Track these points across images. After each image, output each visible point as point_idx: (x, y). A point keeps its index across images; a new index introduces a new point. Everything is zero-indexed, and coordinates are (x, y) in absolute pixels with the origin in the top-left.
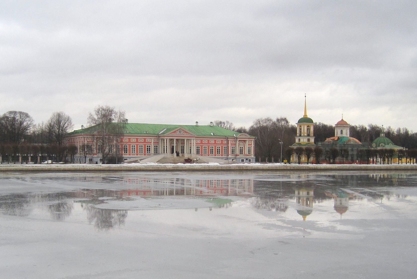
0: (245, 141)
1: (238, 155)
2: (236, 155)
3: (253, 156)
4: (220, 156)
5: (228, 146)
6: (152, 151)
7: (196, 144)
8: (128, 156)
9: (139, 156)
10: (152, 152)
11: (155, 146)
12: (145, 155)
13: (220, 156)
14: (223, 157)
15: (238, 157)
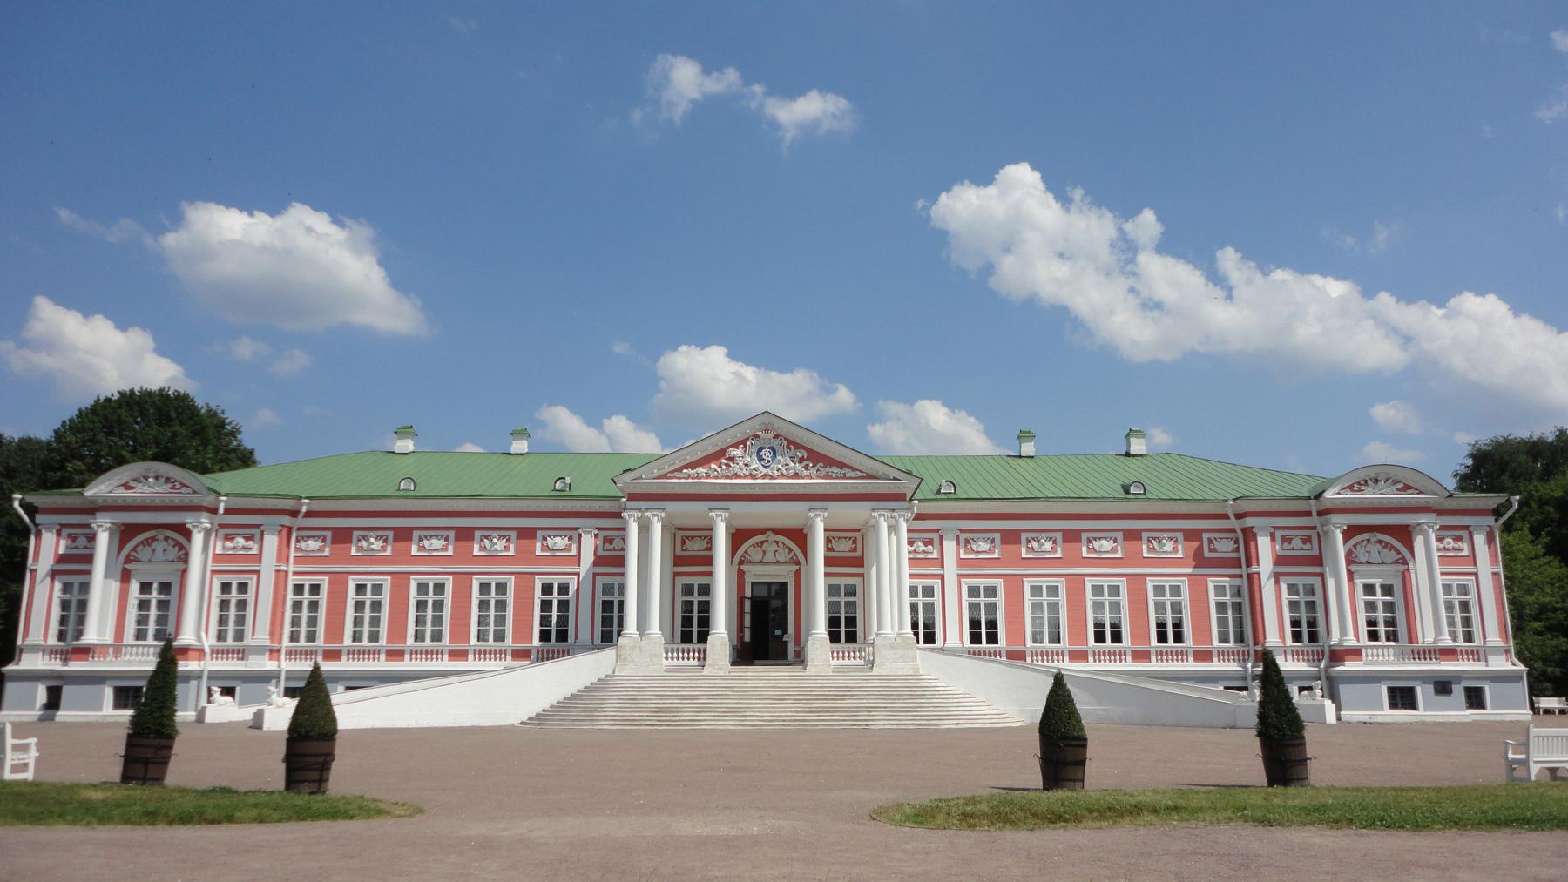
0: (1404, 534)
1: (1356, 653)
2: (1337, 655)
3: (1501, 663)
4: (1191, 666)
5: (1252, 579)
6: (584, 621)
7: (962, 563)
8: (382, 665)
9: (470, 664)
10: (584, 635)
11: (608, 589)
12: (521, 654)
13: (1191, 666)
14: (1216, 666)
15: (1350, 666)
